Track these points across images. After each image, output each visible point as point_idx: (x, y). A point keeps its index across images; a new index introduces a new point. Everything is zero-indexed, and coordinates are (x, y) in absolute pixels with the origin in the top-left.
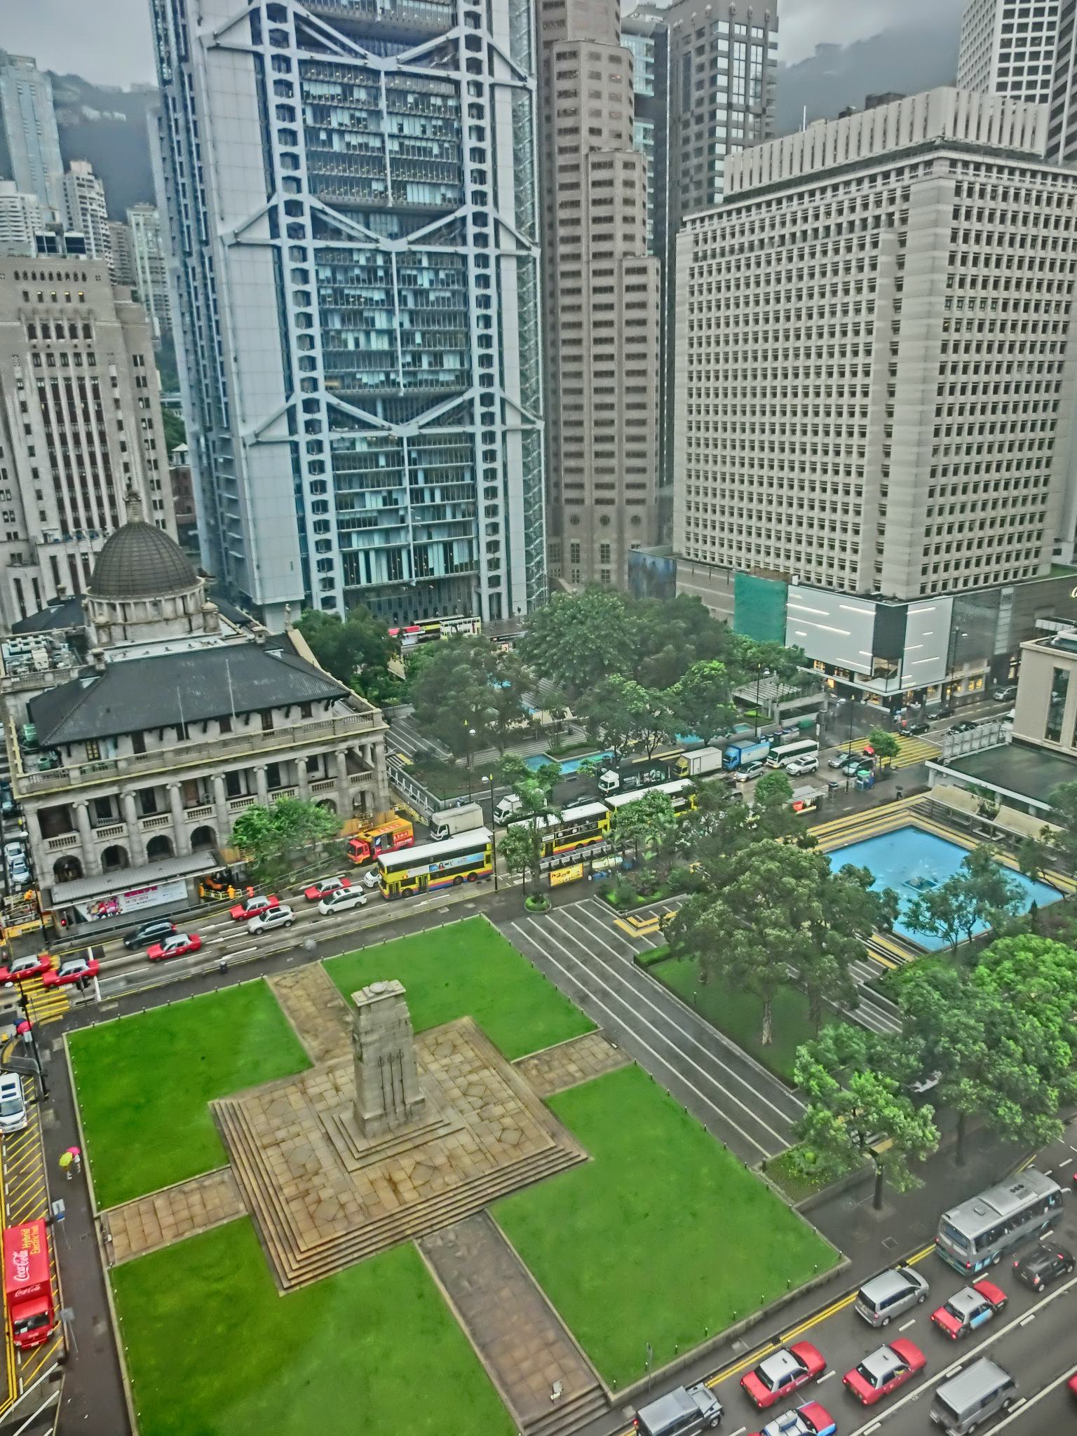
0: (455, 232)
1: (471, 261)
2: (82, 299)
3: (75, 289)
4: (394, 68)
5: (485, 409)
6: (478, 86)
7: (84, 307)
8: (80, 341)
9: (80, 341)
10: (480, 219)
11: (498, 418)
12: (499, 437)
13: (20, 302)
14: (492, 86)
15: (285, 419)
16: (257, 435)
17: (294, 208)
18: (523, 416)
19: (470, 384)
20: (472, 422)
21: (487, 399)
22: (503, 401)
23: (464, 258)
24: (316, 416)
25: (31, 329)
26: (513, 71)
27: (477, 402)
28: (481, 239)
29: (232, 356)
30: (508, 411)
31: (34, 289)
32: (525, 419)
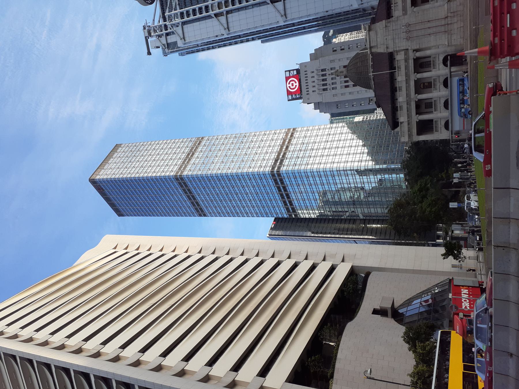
2: (313, 72)
3: (310, 75)
7: (316, 72)
8: (327, 72)
9: (327, 72)
13: (316, 93)
25: (324, 90)
31: (311, 89)
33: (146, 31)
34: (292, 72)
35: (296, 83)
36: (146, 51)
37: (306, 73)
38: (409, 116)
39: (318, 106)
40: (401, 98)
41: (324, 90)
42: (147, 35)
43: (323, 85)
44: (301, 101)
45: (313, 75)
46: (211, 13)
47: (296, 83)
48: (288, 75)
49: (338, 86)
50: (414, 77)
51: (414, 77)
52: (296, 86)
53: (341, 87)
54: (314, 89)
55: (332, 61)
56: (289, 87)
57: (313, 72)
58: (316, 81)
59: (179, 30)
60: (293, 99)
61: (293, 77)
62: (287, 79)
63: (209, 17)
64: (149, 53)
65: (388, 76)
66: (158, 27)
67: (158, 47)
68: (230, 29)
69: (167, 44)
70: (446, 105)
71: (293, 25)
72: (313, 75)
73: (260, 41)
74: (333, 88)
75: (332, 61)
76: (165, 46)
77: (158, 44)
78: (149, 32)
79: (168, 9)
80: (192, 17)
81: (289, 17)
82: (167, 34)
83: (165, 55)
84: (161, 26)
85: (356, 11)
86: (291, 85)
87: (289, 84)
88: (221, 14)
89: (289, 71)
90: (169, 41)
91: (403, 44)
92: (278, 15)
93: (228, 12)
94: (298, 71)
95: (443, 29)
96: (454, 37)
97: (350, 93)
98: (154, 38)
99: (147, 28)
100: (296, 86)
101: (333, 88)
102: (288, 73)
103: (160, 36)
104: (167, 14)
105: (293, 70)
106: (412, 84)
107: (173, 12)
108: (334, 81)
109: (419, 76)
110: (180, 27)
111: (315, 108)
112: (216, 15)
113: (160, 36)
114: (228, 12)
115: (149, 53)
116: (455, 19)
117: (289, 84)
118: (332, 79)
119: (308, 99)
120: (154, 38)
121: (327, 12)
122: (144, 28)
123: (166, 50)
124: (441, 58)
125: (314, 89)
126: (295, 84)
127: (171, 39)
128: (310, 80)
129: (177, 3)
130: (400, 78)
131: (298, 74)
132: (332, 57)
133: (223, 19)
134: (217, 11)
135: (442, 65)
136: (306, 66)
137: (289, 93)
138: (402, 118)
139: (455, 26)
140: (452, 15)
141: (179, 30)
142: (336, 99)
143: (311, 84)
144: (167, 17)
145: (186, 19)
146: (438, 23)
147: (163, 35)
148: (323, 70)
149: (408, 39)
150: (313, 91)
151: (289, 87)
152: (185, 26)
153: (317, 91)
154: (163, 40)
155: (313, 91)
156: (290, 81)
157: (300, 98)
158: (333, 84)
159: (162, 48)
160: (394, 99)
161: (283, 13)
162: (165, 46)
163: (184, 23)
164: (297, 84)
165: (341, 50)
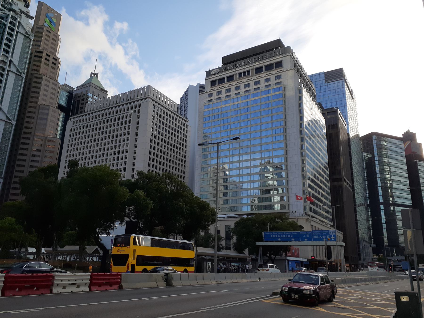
26: (7, 117)
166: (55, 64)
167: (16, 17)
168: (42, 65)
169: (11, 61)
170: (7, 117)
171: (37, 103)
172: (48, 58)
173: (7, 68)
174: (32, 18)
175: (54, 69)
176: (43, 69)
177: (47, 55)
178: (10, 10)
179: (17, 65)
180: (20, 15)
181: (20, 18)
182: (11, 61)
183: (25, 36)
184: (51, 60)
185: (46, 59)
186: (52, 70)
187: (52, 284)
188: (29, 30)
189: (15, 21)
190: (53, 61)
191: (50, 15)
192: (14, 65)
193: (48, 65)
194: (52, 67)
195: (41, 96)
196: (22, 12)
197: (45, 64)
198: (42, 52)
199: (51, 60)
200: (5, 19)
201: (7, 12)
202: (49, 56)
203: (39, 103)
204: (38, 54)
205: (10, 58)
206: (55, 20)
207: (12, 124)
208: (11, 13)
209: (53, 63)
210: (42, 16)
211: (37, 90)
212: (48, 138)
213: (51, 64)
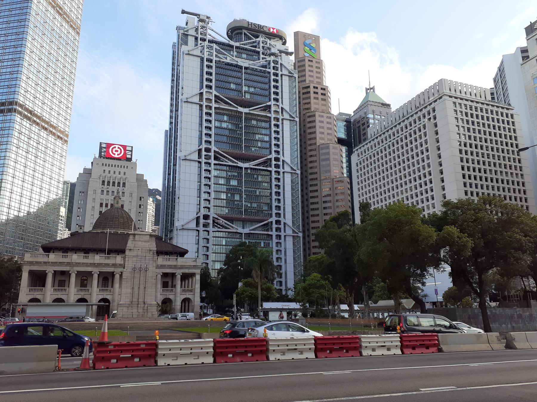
0: (267, 163)
1: (273, 173)
2: (125, 173)
3: (122, 170)
4: (248, 112)
5: (277, 226)
6: (278, 120)
7: (124, 177)
8: (121, 188)
9: (121, 188)
10: (277, 159)
11: (282, 230)
12: (283, 237)
13: (102, 173)
14: (282, 120)
15: (195, 221)
16: (183, 226)
17: (208, 150)
18: (293, 230)
19: (271, 216)
20: (272, 231)
21: (278, 222)
22: (285, 223)
23: (270, 171)
24: (208, 221)
25: (103, 182)
27: (274, 223)
28: (277, 166)
29: (178, 196)
30: (287, 227)
31: (107, 169)
32: (294, 232)
33: (205, 18)
34: (130, 153)
35: (118, 155)
36: (186, 10)
37: (126, 167)
38: (54, 264)
39: (87, 173)
40: (75, 258)
41: (103, 182)
42: (201, 17)
43: (109, 182)
44: (97, 156)
45: (122, 174)
46: (205, 90)
47: (118, 155)
48: (128, 148)
49: (104, 197)
50: (96, 271)
51: (96, 271)
52: (115, 154)
53: (102, 199)
54: (107, 172)
55: (131, 195)
56: (115, 147)
57: (125, 173)
58: (115, 176)
59: (197, 52)
60: (101, 148)
61: (125, 154)
62: (124, 147)
63: (201, 87)
64: (183, 12)
65: (103, 247)
66: (205, 31)
67: (187, 24)
68: (186, 104)
69: (187, 35)
70: (59, 300)
71: (175, 165)
72: (122, 174)
73: (168, 129)
74: (103, 191)
75: (131, 195)
76: (186, 31)
77: (190, 26)
78: (203, 20)
79: (219, 48)
80: (206, 69)
81: (183, 163)
82: (196, 38)
83: (178, 28)
84: (206, 35)
85: (172, 224)
86: (117, 149)
87: (118, 148)
88: (201, 99)
89: (131, 151)
90: (189, 37)
91: (129, 264)
92: (188, 153)
93: (201, 106)
94: (130, 160)
95: (135, 300)
96: (125, 310)
97: (93, 207)
98: (196, 24)
99: (207, 20)
100: (115, 154)
101: (103, 191)
102: (130, 149)
103: (197, 30)
104: (215, 46)
105: (131, 155)
106: (89, 269)
107: (215, 53)
108: (110, 193)
109: (96, 276)
110: (200, 54)
111: (85, 169)
112: (201, 94)
113: (197, 30)
114: (201, 106)
115: (183, 12)
116: (141, 311)
117: (118, 148)
118: (113, 192)
119: (98, 164)
120: (196, 24)
121: (179, 198)
122: (208, 18)
123: (182, 31)
124: (108, 297)
125: (107, 172)
126: (116, 153)
127: (191, 40)
128: (117, 170)
129: (221, 60)
130: (97, 258)
131: (126, 159)
132: (135, 195)
133: (196, 99)
134: (205, 96)
135: (101, 297)
136: (132, 168)
137: (109, 145)
138: (53, 257)
139: (135, 311)
140: (146, 308)
141: (197, 52)
142: (90, 192)
143: (112, 169)
144: (212, 45)
145: (206, 63)
146: (141, 295)
147: (197, 34)
148: (124, 184)
149: (134, 269)
150: (104, 171)
151: (115, 147)
152: (199, 59)
153: (104, 175)
154: (192, 32)
155: (104, 171)
156: (121, 150)
157: (100, 156)
158: (108, 191)
159: (184, 28)
160: (76, 250)
161: (188, 158)
162: (186, 31)
163: (202, 59)
164: (116, 156)
165: (140, 205)
166: (325, 95)
167: (277, 60)
168: (313, 101)
169: (282, 108)
170: (291, 168)
171: (315, 144)
172: (316, 90)
173: (281, 117)
174: (291, 54)
175: (325, 100)
176: (314, 105)
177: (314, 87)
178: (270, 55)
179: (288, 111)
180: (280, 56)
181: (281, 59)
182: (282, 108)
183: (289, 76)
184: (320, 91)
185: (314, 93)
186: (323, 102)
187: (267, 350)
188: (291, 68)
189: (277, 64)
190: (322, 91)
191: (308, 42)
192: (286, 111)
193: (317, 99)
194: (322, 99)
195: (318, 136)
196: (281, 52)
197: (315, 98)
198: (309, 87)
199: (320, 91)
200: (268, 67)
201: (268, 58)
202: (317, 88)
203: (318, 144)
204: (305, 91)
205: (281, 106)
206: (313, 45)
207: (298, 174)
208: (272, 58)
209: (322, 94)
210: (301, 46)
211: (312, 130)
212: (335, 180)
213: (320, 96)
